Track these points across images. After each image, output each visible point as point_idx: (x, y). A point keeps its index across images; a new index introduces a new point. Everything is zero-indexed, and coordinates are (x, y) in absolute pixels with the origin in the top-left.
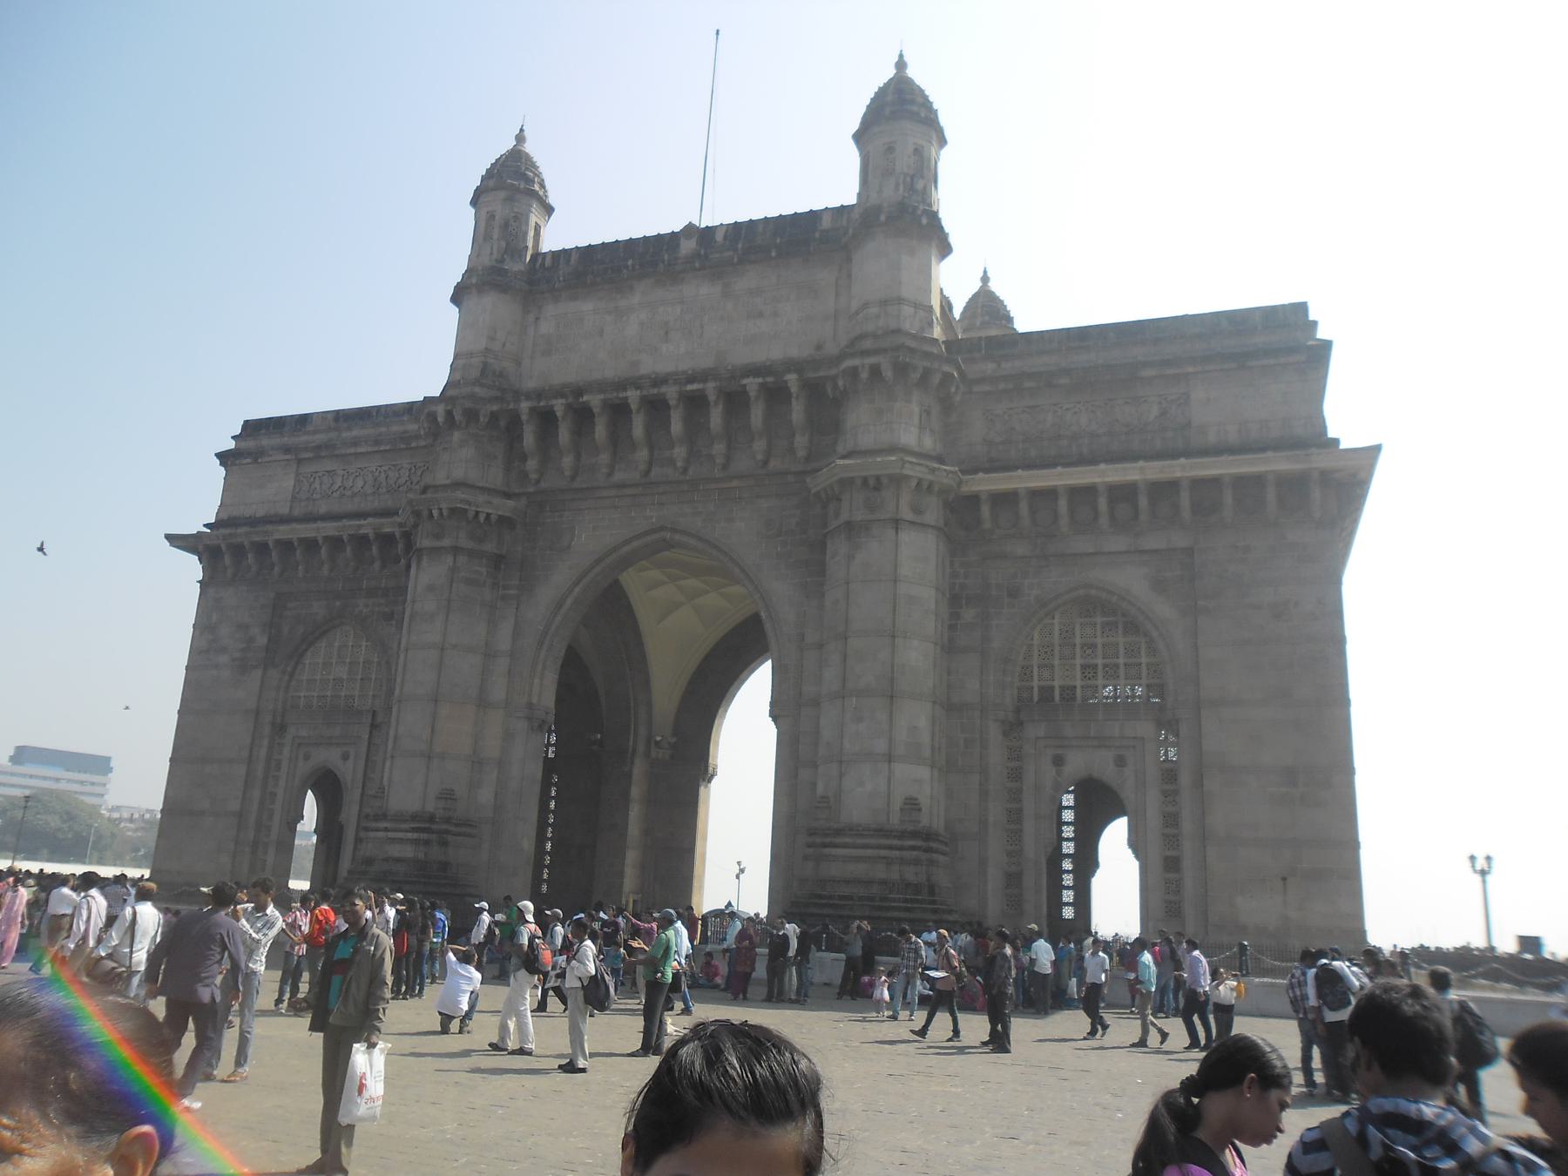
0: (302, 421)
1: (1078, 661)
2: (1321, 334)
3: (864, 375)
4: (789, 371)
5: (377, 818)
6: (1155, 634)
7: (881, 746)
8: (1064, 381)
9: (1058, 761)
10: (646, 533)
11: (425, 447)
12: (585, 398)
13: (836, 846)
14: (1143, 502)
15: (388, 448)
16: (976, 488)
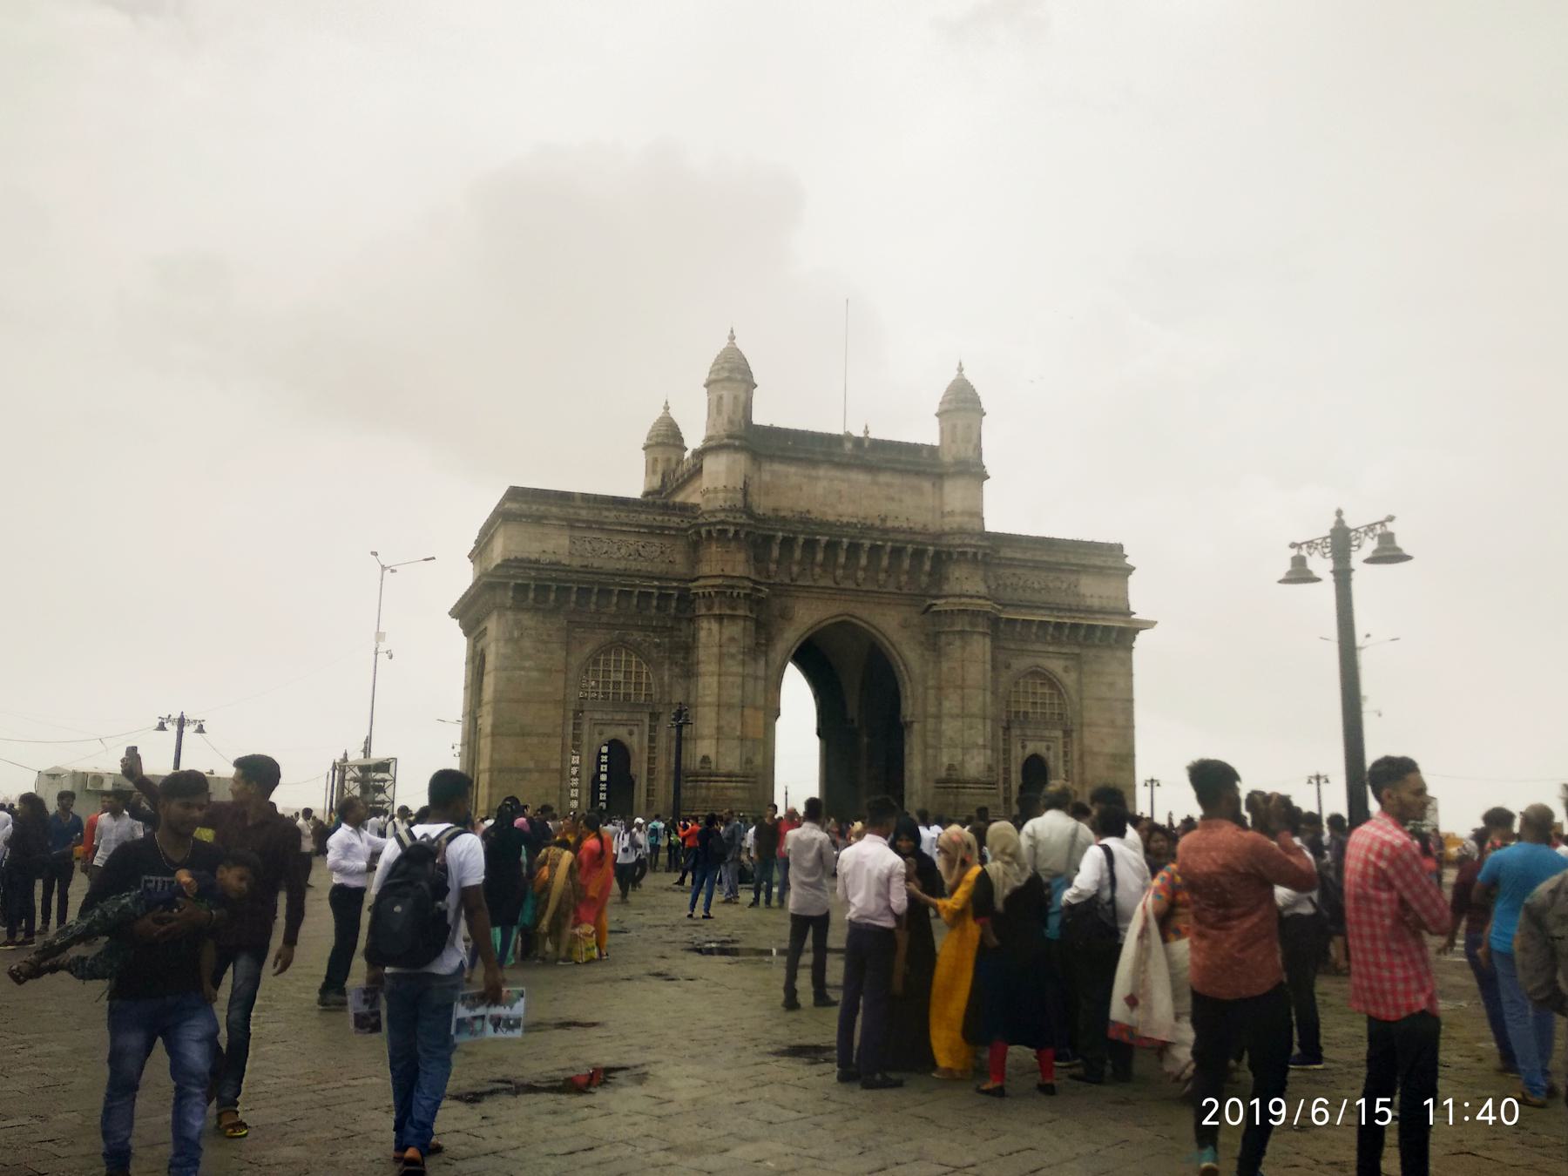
0: (565, 497)
1: (1030, 700)
2: (1128, 561)
3: (969, 556)
4: (930, 545)
5: (710, 775)
6: (1063, 690)
7: (981, 741)
8: (1030, 564)
9: (1024, 747)
10: (836, 616)
11: (673, 535)
12: (818, 537)
13: (964, 788)
14: (1066, 631)
15: (646, 531)
16: (1002, 616)
